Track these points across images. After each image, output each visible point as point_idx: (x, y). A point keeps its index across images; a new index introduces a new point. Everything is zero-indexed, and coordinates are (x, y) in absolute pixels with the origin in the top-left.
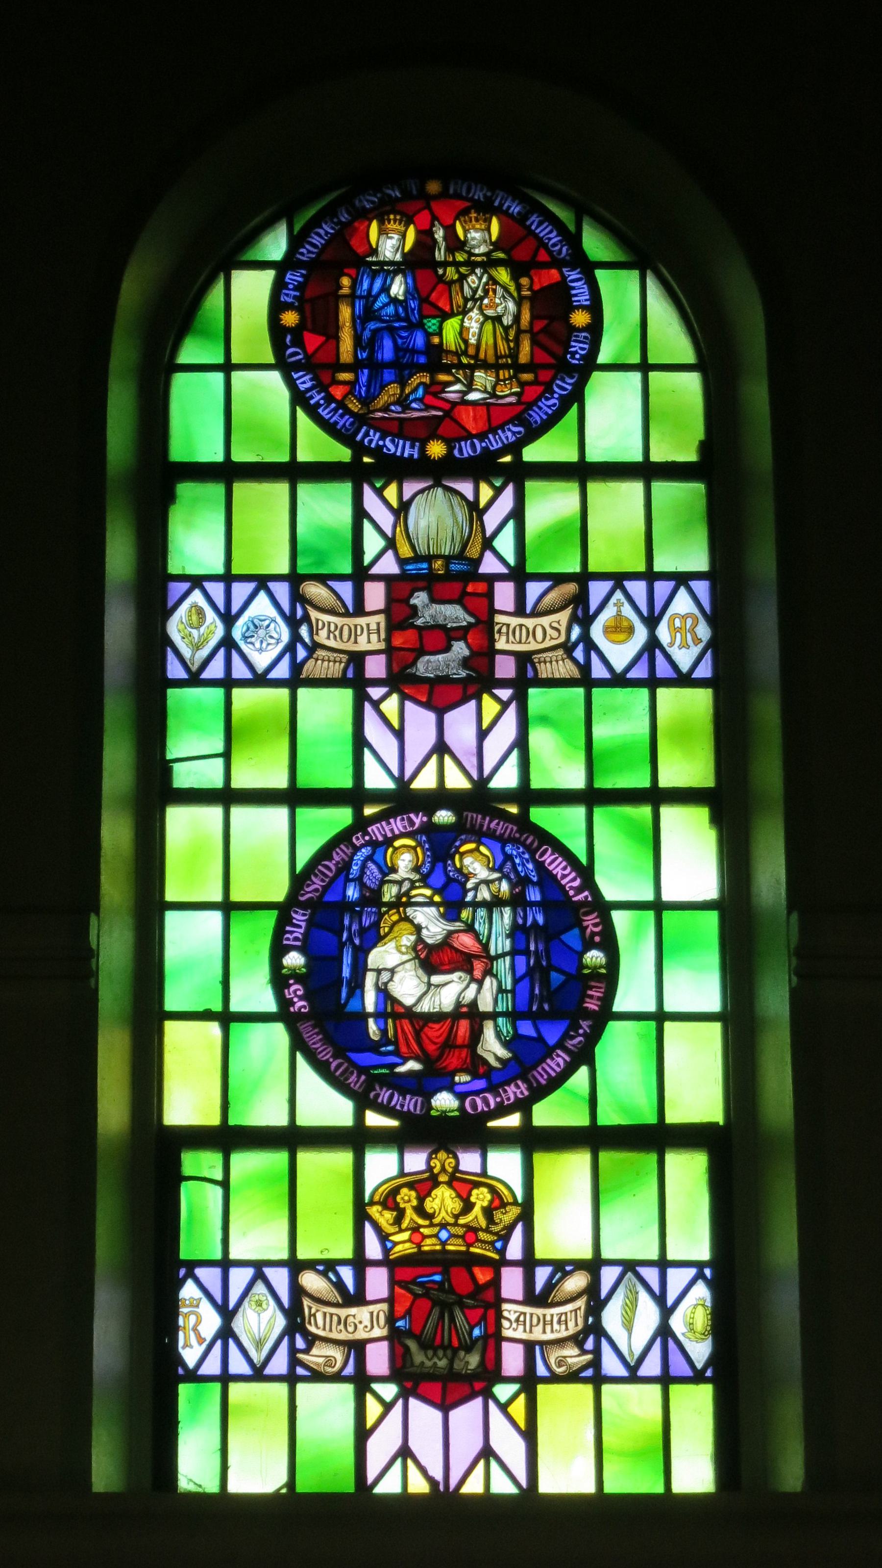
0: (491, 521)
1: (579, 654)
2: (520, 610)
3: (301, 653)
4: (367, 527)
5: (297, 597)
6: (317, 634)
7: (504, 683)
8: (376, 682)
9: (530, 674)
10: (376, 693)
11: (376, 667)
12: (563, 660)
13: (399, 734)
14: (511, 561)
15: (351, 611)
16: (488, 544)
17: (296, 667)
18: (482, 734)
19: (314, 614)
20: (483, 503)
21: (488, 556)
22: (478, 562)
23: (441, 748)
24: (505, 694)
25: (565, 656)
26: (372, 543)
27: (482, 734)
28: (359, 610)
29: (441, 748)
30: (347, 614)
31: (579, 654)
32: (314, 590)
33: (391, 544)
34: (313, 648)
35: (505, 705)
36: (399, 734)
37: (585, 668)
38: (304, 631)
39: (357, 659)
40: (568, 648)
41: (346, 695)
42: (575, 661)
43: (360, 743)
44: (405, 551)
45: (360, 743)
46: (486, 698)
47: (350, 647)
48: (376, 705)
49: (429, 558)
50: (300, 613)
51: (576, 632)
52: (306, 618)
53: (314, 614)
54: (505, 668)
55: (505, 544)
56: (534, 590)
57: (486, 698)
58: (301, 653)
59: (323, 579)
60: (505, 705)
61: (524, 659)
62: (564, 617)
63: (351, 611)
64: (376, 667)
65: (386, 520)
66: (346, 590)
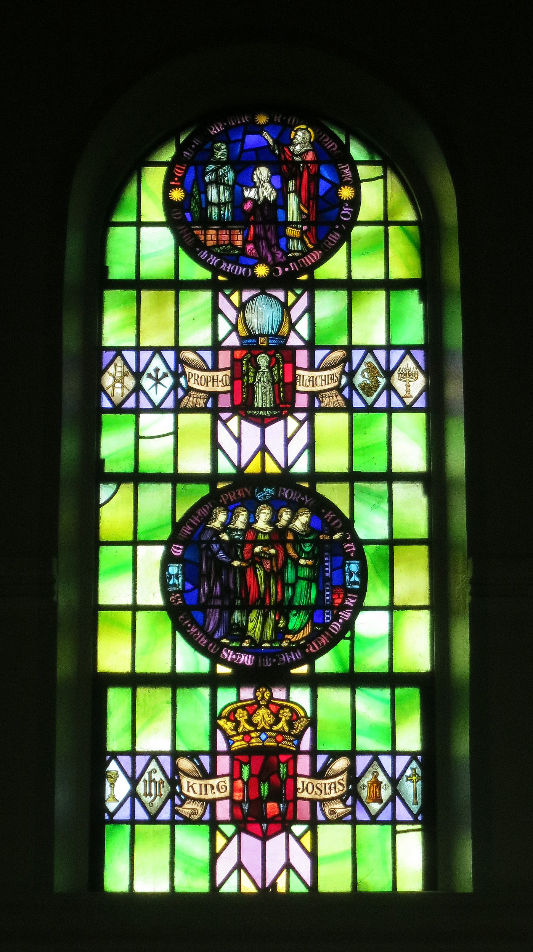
0: (295, 313)
1: (346, 393)
2: (311, 367)
3: (181, 393)
4: (220, 318)
5: (179, 360)
6: (189, 381)
7: (301, 410)
8: (225, 410)
9: (317, 405)
10: (224, 416)
11: (225, 401)
12: (336, 396)
13: (238, 440)
14: (306, 337)
15: (210, 366)
16: (292, 327)
17: (178, 401)
18: (287, 441)
19: (188, 370)
20: (290, 303)
21: (292, 333)
22: (287, 337)
23: (263, 449)
24: (301, 416)
25: (337, 394)
26: (224, 328)
27: (287, 441)
28: (215, 368)
29: (263, 449)
30: (208, 370)
31: (346, 393)
32: (189, 355)
33: (235, 328)
34: (188, 390)
35: (301, 423)
36: (238, 440)
37: (349, 401)
38: (182, 380)
39: (214, 395)
40: (339, 389)
41: (207, 418)
42: (343, 397)
43: (216, 446)
44: (244, 333)
45: (216, 446)
46: (289, 418)
47: (210, 388)
48: (225, 422)
49: (257, 337)
50: (180, 370)
51: (344, 380)
52: (184, 373)
53: (188, 370)
54: (302, 401)
55: (303, 327)
56: (319, 355)
57: (289, 418)
58: (181, 393)
59: (194, 349)
60: (301, 423)
61: (312, 395)
62: (337, 371)
63: (210, 366)
64: (225, 401)
65: (232, 314)
66: (207, 356)
